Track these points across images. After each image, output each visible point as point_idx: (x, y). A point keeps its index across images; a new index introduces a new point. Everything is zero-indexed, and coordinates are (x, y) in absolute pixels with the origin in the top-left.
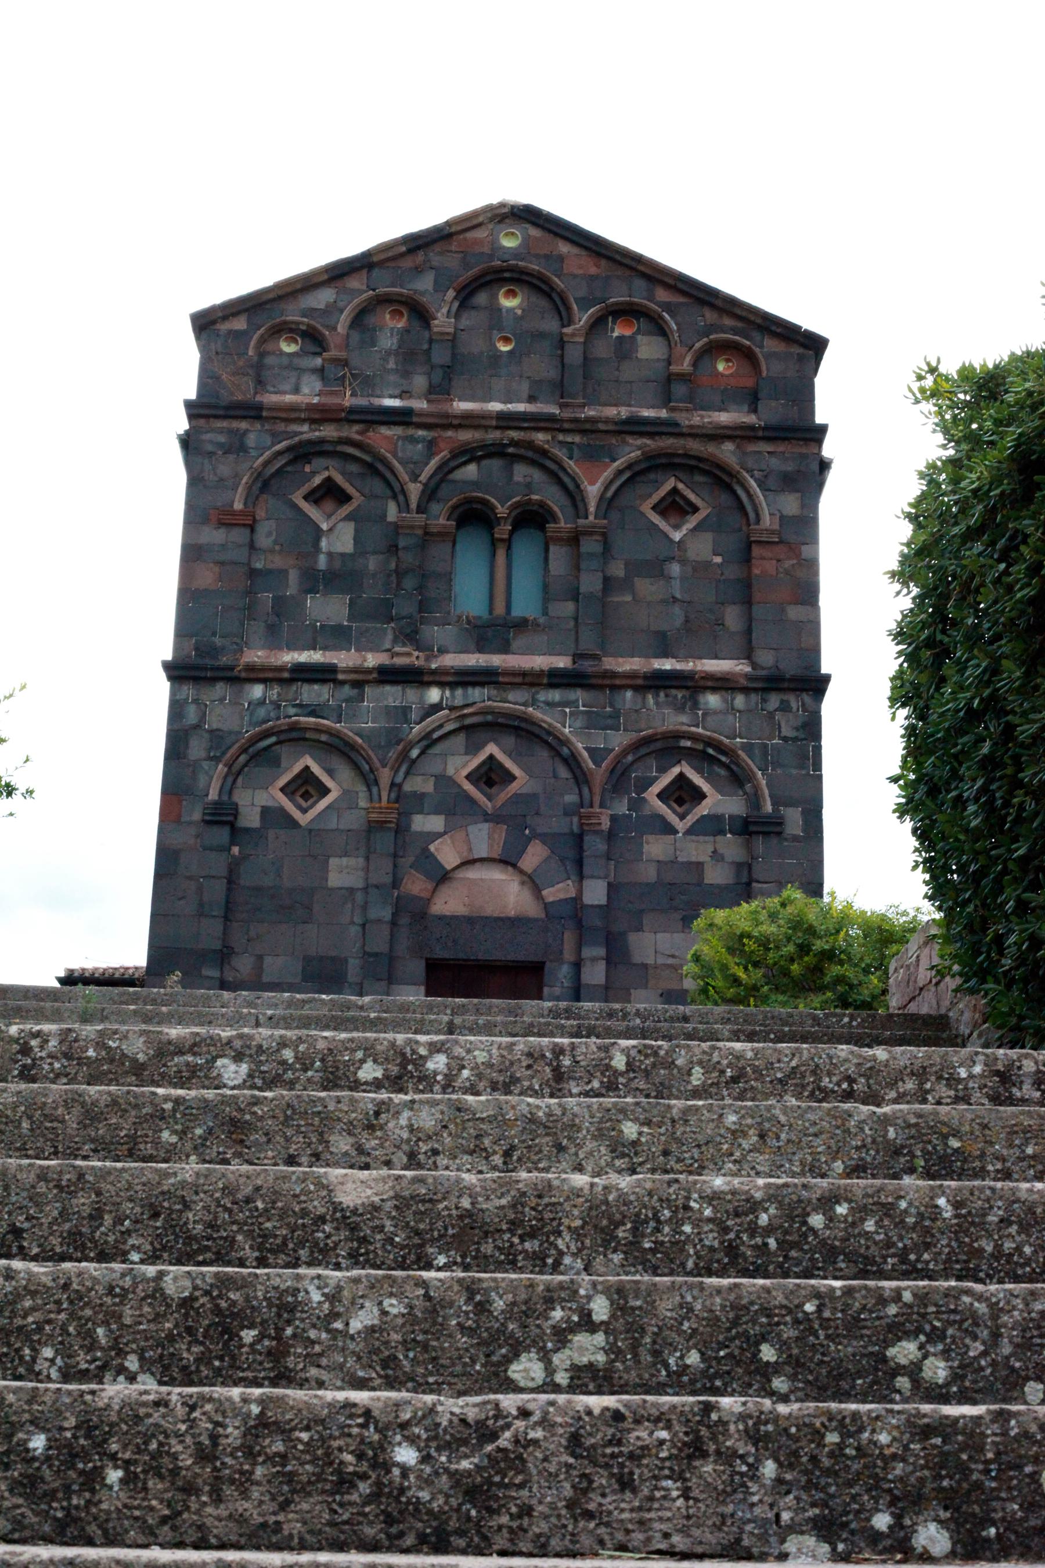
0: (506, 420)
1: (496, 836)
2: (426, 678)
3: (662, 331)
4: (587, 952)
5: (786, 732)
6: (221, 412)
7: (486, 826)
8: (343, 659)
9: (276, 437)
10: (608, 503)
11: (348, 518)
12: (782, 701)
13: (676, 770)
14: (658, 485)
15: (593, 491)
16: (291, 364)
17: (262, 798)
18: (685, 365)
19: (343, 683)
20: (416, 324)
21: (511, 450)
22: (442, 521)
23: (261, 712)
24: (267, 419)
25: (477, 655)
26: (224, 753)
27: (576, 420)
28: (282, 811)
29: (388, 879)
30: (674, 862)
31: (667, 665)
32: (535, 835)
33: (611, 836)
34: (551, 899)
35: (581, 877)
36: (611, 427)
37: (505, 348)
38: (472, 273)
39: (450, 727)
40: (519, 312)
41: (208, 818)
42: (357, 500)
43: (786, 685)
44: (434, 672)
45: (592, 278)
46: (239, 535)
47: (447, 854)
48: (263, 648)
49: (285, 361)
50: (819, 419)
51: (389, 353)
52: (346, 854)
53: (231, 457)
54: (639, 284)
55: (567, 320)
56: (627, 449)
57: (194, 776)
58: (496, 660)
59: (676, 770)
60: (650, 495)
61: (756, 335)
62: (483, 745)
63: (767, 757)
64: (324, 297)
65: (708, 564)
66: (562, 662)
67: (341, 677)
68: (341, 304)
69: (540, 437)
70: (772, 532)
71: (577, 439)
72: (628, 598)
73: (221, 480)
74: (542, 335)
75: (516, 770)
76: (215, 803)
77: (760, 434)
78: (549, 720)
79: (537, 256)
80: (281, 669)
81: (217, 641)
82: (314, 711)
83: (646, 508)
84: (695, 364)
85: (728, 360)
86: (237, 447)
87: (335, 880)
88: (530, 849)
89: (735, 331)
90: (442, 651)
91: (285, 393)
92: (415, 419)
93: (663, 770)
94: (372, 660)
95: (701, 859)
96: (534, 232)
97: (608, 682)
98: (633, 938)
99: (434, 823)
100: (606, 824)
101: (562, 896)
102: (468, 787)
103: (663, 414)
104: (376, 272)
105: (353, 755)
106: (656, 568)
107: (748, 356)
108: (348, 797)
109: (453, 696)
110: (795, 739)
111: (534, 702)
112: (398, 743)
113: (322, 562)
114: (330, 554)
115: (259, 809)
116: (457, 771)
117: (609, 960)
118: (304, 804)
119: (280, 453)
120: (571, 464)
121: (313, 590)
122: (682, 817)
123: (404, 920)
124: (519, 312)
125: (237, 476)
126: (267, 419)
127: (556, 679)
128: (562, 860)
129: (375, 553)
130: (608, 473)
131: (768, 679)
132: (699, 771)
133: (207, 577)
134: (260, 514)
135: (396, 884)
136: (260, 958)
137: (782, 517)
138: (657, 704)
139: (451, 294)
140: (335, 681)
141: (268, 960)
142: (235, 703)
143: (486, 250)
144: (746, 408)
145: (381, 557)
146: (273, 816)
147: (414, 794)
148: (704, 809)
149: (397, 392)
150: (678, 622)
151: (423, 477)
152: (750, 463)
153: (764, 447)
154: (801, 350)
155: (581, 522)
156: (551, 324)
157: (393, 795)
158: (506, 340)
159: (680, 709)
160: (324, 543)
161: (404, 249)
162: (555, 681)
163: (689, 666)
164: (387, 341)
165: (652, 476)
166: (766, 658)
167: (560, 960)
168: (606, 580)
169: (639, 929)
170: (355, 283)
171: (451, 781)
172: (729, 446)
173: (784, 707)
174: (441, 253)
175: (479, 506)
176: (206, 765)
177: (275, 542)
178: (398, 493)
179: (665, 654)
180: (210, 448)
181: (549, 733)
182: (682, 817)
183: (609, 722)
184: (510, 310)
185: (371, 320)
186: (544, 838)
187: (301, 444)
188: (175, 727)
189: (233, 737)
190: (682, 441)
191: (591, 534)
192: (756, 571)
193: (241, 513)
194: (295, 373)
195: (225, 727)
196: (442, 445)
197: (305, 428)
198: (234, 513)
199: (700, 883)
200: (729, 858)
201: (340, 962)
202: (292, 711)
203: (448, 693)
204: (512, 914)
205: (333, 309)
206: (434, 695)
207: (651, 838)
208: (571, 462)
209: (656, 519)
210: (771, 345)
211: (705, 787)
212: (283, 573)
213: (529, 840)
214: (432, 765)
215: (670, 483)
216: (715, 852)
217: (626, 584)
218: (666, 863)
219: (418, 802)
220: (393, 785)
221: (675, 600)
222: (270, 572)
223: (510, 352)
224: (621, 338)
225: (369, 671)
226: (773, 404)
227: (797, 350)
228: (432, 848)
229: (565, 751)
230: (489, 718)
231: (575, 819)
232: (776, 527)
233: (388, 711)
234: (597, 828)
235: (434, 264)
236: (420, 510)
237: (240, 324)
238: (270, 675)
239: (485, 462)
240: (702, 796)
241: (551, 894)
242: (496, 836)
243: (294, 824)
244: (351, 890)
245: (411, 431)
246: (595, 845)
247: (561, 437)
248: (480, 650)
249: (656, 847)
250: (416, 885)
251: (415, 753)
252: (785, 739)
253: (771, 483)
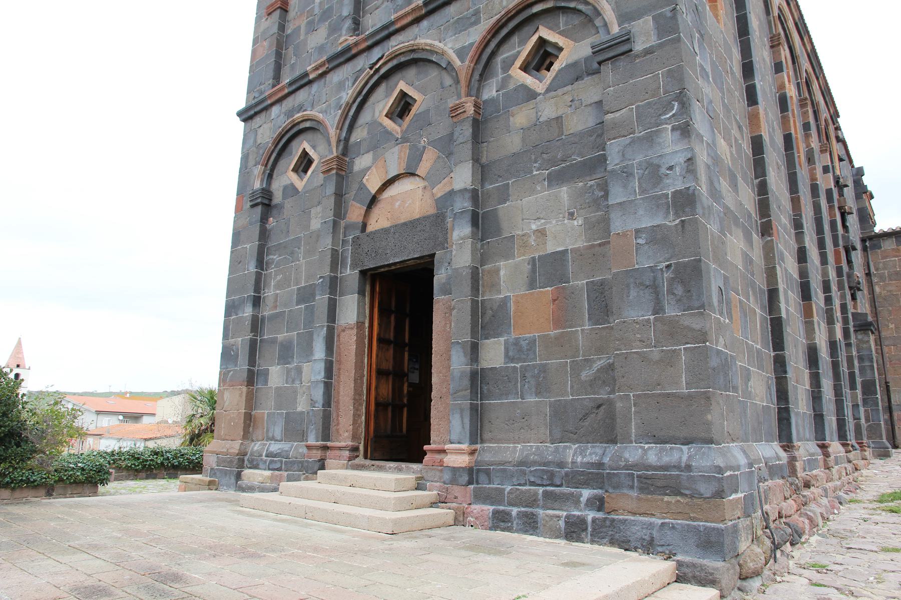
1: (402, 154)
7: (397, 147)
34: (439, 195)
41: (251, 204)
59: (535, 38)
67: (311, 77)
78: (429, 41)
93: (523, 42)
102: (388, 123)
115: (281, 189)
116: (381, 112)
181: (432, 52)
183: (473, 19)
204: (417, 217)
207: (514, 109)
214: (365, 117)
218: (529, 129)
220: (339, 141)
230: (395, 62)
234: (465, 115)
242: (402, 154)
249: (521, 117)
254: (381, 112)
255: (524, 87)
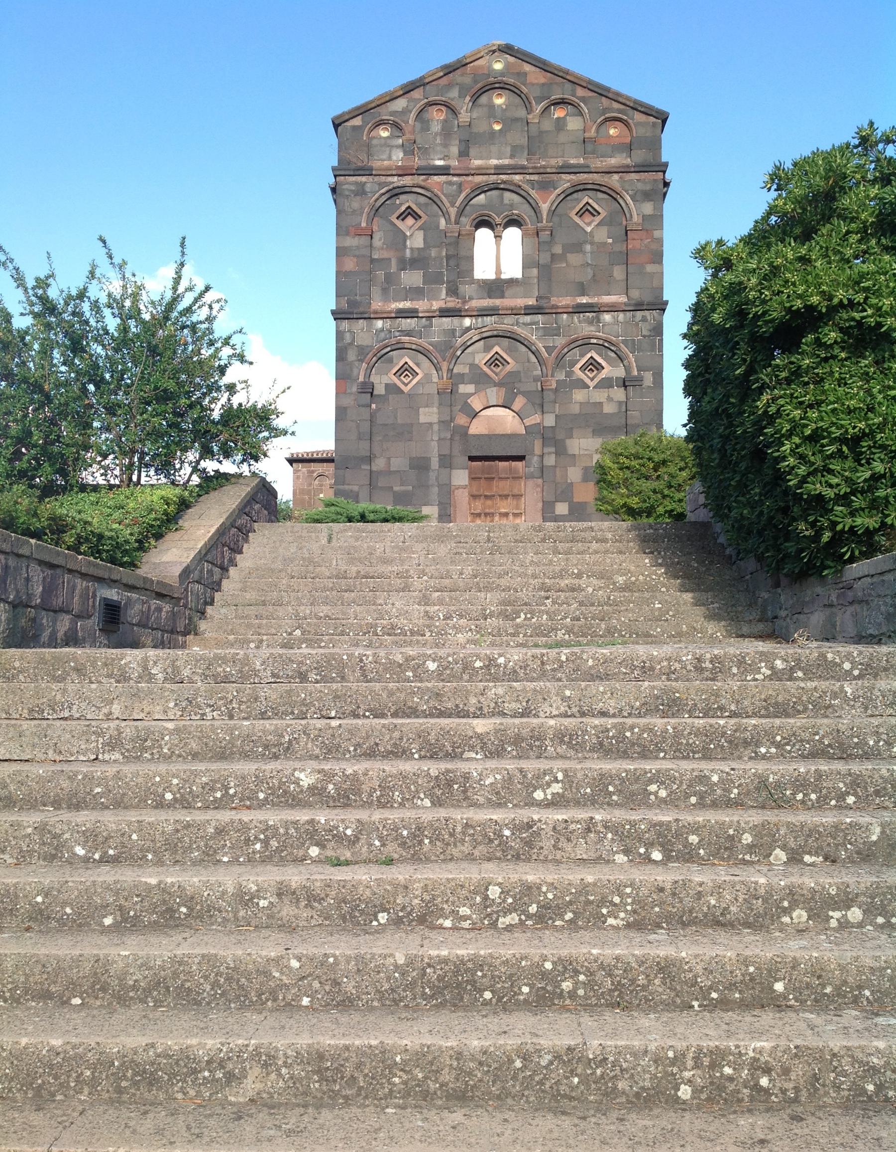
0: (499, 170)
2: (463, 314)
3: (581, 114)
4: (546, 450)
5: (645, 333)
6: (352, 173)
8: (421, 305)
9: (381, 185)
10: (552, 213)
11: (420, 228)
12: (643, 316)
13: (589, 356)
14: (578, 200)
15: (545, 207)
16: (386, 144)
17: (385, 380)
18: (592, 133)
19: (422, 317)
20: (450, 116)
21: (502, 186)
22: (468, 227)
23: (382, 335)
24: (376, 175)
25: (488, 300)
26: (365, 357)
27: (535, 168)
28: (395, 385)
29: (448, 418)
30: (588, 403)
31: (584, 300)
32: (520, 392)
33: (556, 390)
35: (543, 412)
36: (554, 170)
37: (497, 127)
38: (479, 86)
39: (475, 338)
40: (504, 107)
42: (424, 218)
43: (645, 307)
44: (466, 310)
45: (543, 84)
46: (365, 240)
47: (476, 403)
48: (381, 301)
49: (383, 141)
50: (664, 159)
51: (436, 134)
52: (427, 406)
53: (358, 198)
54: (568, 86)
55: (529, 110)
56: (562, 182)
57: (352, 370)
58: (497, 302)
59: (589, 356)
60: (575, 207)
61: (631, 112)
62: (493, 347)
63: (634, 346)
64: (400, 104)
65: (606, 243)
66: (531, 302)
67: (420, 315)
68: (410, 108)
69: (517, 178)
70: (639, 224)
71: (535, 177)
72: (564, 265)
73: (354, 211)
74: (516, 120)
75: (509, 360)
76: (362, 383)
77: (633, 169)
79: (513, 73)
80: (390, 312)
81: (358, 298)
82: (408, 333)
83: (573, 214)
84: (597, 131)
85: (615, 128)
86: (361, 191)
87: (423, 419)
88: (517, 400)
89: (620, 111)
90: (471, 298)
91: (383, 160)
92: (452, 172)
94: (436, 305)
95: (601, 401)
96: (511, 59)
97: (554, 311)
98: (568, 442)
99: (469, 388)
100: (554, 386)
101: (533, 422)
102: (485, 369)
103: (582, 161)
104: (428, 87)
105: (429, 355)
106: (577, 248)
107: (625, 123)
108: (427, 376)
109: (477, 322)
110: (650, 336)
111: (518, 324)
112: (451, 348)
113: (408, 253)
114: (412, 249)
116: (480, 361)
117: (557, 454)
118: (406, 382)
119: (383, 194)
120: (533, 193)
121: (404, 269)
122: (592, 379)
123: (457, 438)
124: (504, 107)
125: (362, 209)
126: (376, 175)
127: (530, 311)
128: (533, 404)
129: (434, 247)
130: (553, 196)
131: (636, 305)
132: (600, 355)
133: (350, 264)
134: (375, 228)
135: (452, 419)
136: (389, 459)
137: (643, 216)
138: (580, 322)
139: (468, 98)
140: (417, 317)
141: (393, 460)
142: (369, 331)
143: (486, 72)
144: (625, 155)
145: (437, 249)
146: (392, 389)
147: (459, 374)
148: (603, 374)
149: (442, 156)
150: (590, 277)
151: (457, 204)
152: (627, 187)
153: (633, 176)
154: (655, 120)
155: (539, 225)
156: (522, 113)
157: (449, 375)
158: (498, 122)
159: (590, 322)
160: (408, 243)
161: (442, 74)
162: (527, 312)
163: (595, 300)
164: (436, 127)
165: (575, 195)
166: (635, 294)
167: (533, 454)
168: (553, 255)
169: (571, 437)
170: (417, 94)
171: (478, 367)
172: (616, 177)
173: (644, 319)
174: (462, 75)
175: (486, 218)
176: (357, 363)
177: (384, 243)
178: (446, 214)
179: (583, 294)
180: (347, 193)
182: (592, 379)
183: (555, 332)
184: (499, 106)
185: (426, 116)
186: (524, 394)
187: (394, 188)
188: (340, 345)
189: (369, 349)
190: (591, 175)
191: (545, 230)
192: (630, 247)
193: (366, 228)
194: (388, 149)
195: (365, 344)
196: (466, 185)
197: (395, 179)
198: (362, 229)
199: (601, 413)
200: (615, 400)
201: (428, 460)
202: (397, 334)
203: (474, 321)
204: (509, 432)
205: (406, 111)
206: (467, 322)
208: (534, 192)
209: (577, 219)
210: (639, 117)
211: (604, 363)
212: (390, 259)
213: (516, 394)
215: (586, 199)
216: (608, 396)
217: (562, 257)
219: (462, 378)
221: (588, 264)
222: (383, 259)
223: (500, 130)
224: (558, 118)
225: (434, 311)
226: (639, 152)
227: (652, 119)
228: (469, 401)
229: (533, 348)
230: (495, 333)
231: (539, 384)
232: (641, 221)
233: (445, 332)
235: (459, 81)
236: (457, 223)
237: (357, 121)
238: (385, 315)
239: (489, 193)
240: (603, 368)
241: (529, 422)
243: (402, 392)
244: (431, 424)
245: (450, 178)
246: (549, 396)
247: (528, 177)
248: (490, 297)
249: (579, 396)
250: (462, 420)
251: (459, 353)
252: (644, 336)
253: (638, 197)
254: (480, 361)
255: (582, 380)
